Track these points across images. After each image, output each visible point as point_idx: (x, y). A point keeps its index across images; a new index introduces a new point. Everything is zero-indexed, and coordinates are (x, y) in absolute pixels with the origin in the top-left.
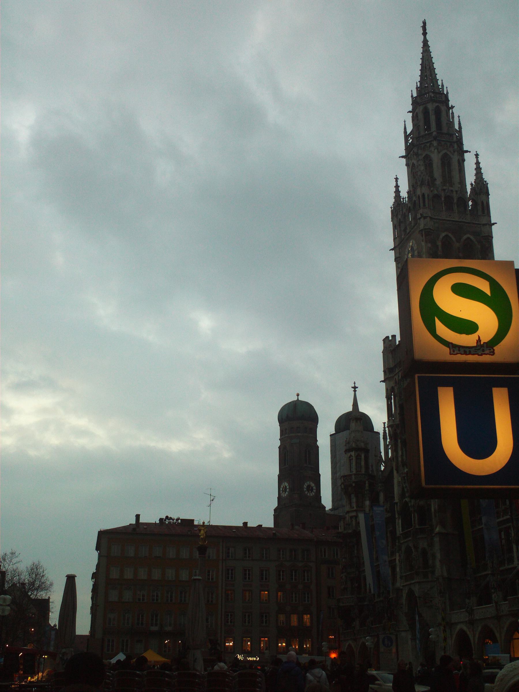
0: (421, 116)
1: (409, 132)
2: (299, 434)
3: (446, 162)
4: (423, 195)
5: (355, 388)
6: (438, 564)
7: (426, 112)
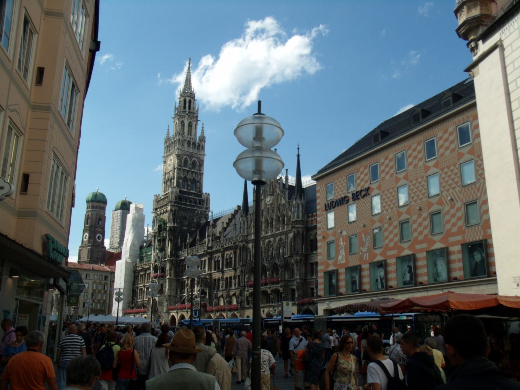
0: (183, 102)
1: (177, 106)
6: (167, 290)
7: (185, 101)
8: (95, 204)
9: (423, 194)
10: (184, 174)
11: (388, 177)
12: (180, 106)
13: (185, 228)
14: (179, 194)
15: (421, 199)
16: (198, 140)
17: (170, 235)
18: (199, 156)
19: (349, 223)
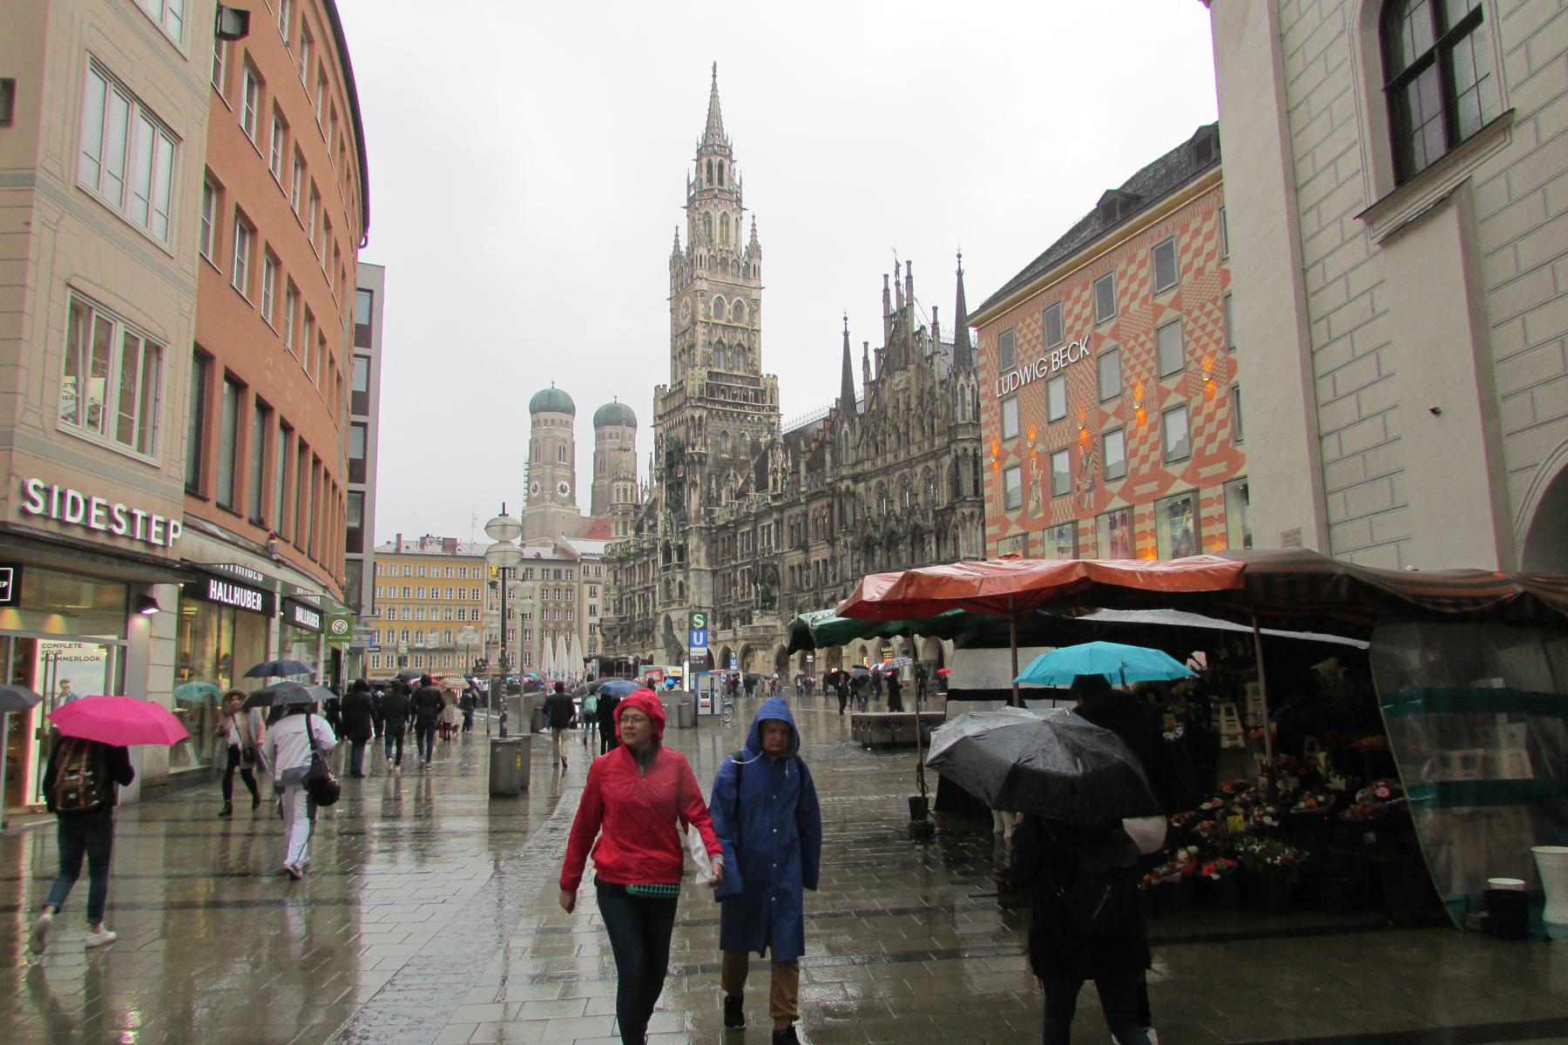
0: (705, 168)
1: (692, 180)
3: (724, 220)
7: (710, 166)
9: (1217, 342)
11: (1135, 306)
12: (698, 178)
15: (1212, 354)
19: (1050, 423)
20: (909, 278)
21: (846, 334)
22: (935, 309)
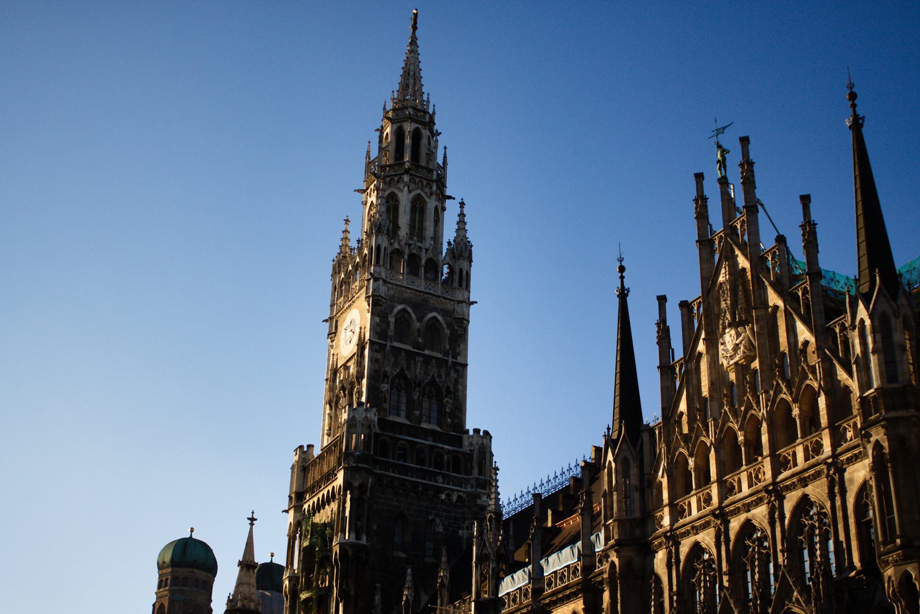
2: (186, 588)
4: (378, 247)
5: (252, 520)
7: (399, 135)
8: (182, 572)
10: (395, 364)
13: (403, 555)
14: (377, 430)
16: (444, 251)
17: (344, 578)
18: (449, 306)
20: (748, 166)
21: (623, 295)
22: (806, 200)
